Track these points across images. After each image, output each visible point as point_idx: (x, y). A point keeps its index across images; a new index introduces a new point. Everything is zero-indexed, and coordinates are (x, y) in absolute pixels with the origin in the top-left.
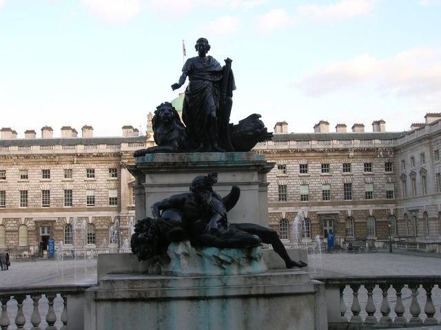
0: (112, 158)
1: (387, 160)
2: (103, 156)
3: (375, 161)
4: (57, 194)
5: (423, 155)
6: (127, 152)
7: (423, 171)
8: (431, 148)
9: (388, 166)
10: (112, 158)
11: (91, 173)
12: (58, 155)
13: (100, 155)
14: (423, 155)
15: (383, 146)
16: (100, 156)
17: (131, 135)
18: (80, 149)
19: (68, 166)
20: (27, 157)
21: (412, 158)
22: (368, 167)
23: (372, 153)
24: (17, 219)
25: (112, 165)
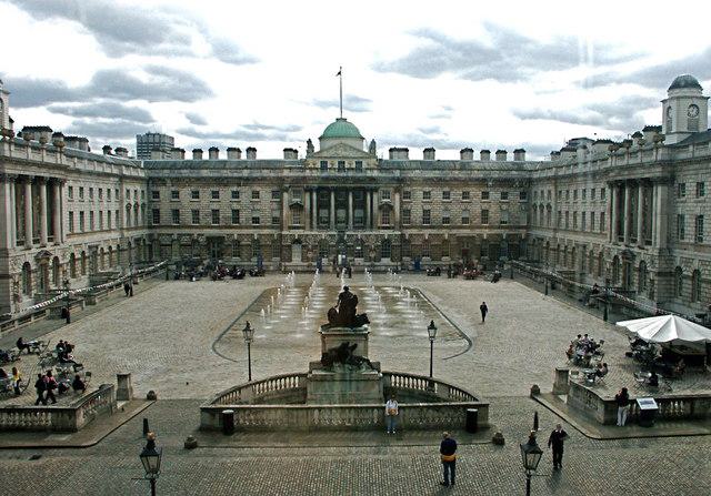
3: (511, 191)
4: (226, 213)
5: (549, 192)
7: (549, 206)
8: (556, 187)
9: (523, 195)
11: (256, 194)
12: (226, 178)
13: (264, 179)
14: (549, 192)
18: (245, 173)
19: (235, 189)
20: (198, 179)
21: (542, 192)
22: (504, 196)
24: (190, 235)
25: (275, 188)
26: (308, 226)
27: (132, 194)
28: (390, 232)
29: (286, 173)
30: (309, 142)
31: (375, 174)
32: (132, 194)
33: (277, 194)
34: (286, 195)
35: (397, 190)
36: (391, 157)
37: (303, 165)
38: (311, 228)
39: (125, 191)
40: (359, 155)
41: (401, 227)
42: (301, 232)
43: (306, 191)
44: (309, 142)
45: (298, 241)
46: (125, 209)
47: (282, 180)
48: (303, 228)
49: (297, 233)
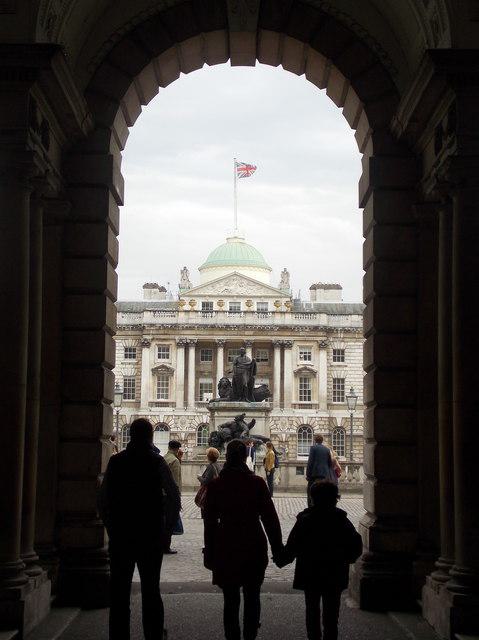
0: (130, 333)
6: (152, 325)
10: (130, 333)
17: (156, 298)
26: (180, 403)
28: (311, 412)
29: (147, 318)
31: (289, 320)
34: (145, 351)
35: (322, 346)
37: (174, 308)
38: (186, 404)
40: (262, 292)
42: (168, 410)
43: (179, 345)
44: (185, 271)
48: (173, 404)
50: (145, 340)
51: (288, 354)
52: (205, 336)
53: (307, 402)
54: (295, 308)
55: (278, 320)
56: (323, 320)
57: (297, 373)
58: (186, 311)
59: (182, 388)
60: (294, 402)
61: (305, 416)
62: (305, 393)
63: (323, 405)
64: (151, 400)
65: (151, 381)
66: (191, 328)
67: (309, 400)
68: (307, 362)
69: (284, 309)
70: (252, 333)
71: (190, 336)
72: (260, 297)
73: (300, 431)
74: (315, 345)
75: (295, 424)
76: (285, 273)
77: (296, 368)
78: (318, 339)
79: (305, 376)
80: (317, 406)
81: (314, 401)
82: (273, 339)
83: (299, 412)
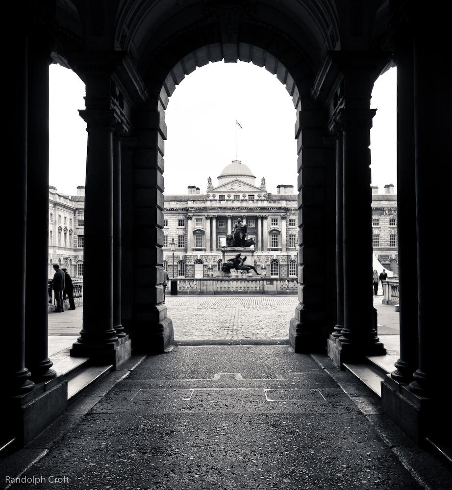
0: (181, 212)
1: (391, 217)
2: (174, 210)
6: (192, 208)
10: (181, 212)
15: (388, 206)
16: (171, 210)
17: (195, 193)
23: (380, 212)
25: (181, 217)
26: (208, 248)
27: (63, 219)
28: (278, 253)
29: (190, 204)
30: (210, 179)
31: (266, 204)
32: (63, 219)
33: (181, 223)
34: (189, 222)
35: (284, 218)
36: (279, 192)
37: (204, 199)
38: (212, 250)
39: (57, 216)
40: (251, 189)
41: (288, 250)
42: (202, 253)
43: (207, 218)
44: (210, 179)
45: (200, 261)
46: (57, 231)
47: (186, 210)
48: (205, 250)
49: (199, 254)
50: (189, 216)
51: (265, 222)
52: (221, 213)
53: (276, 247)
54: (269, 198)
55: (260, 204)
56: (283, 204)
57: (270, 233)
58: (210, 200)
59: (209, 241)
60: (269, 247)
61: (275, 254)
62: (275, 243)
63: (284, 249)
64: (193, 248)
65: (193, 238)
66: (213, 209)
67: (277, 246)
68: (276, 226)
69: (263, 198)
70: (246, 211)
71: (212, 214)
72: (250, 192)
73: (272, 262)
74: (279, 217)
75: (269, 259)
76: (263, 180)
77: (270, 230)
78: (282, 214)
79: (275, 233)
80: (281, 250)
81: (279, 247)
82: (257, 214)
83: (272, 253)
